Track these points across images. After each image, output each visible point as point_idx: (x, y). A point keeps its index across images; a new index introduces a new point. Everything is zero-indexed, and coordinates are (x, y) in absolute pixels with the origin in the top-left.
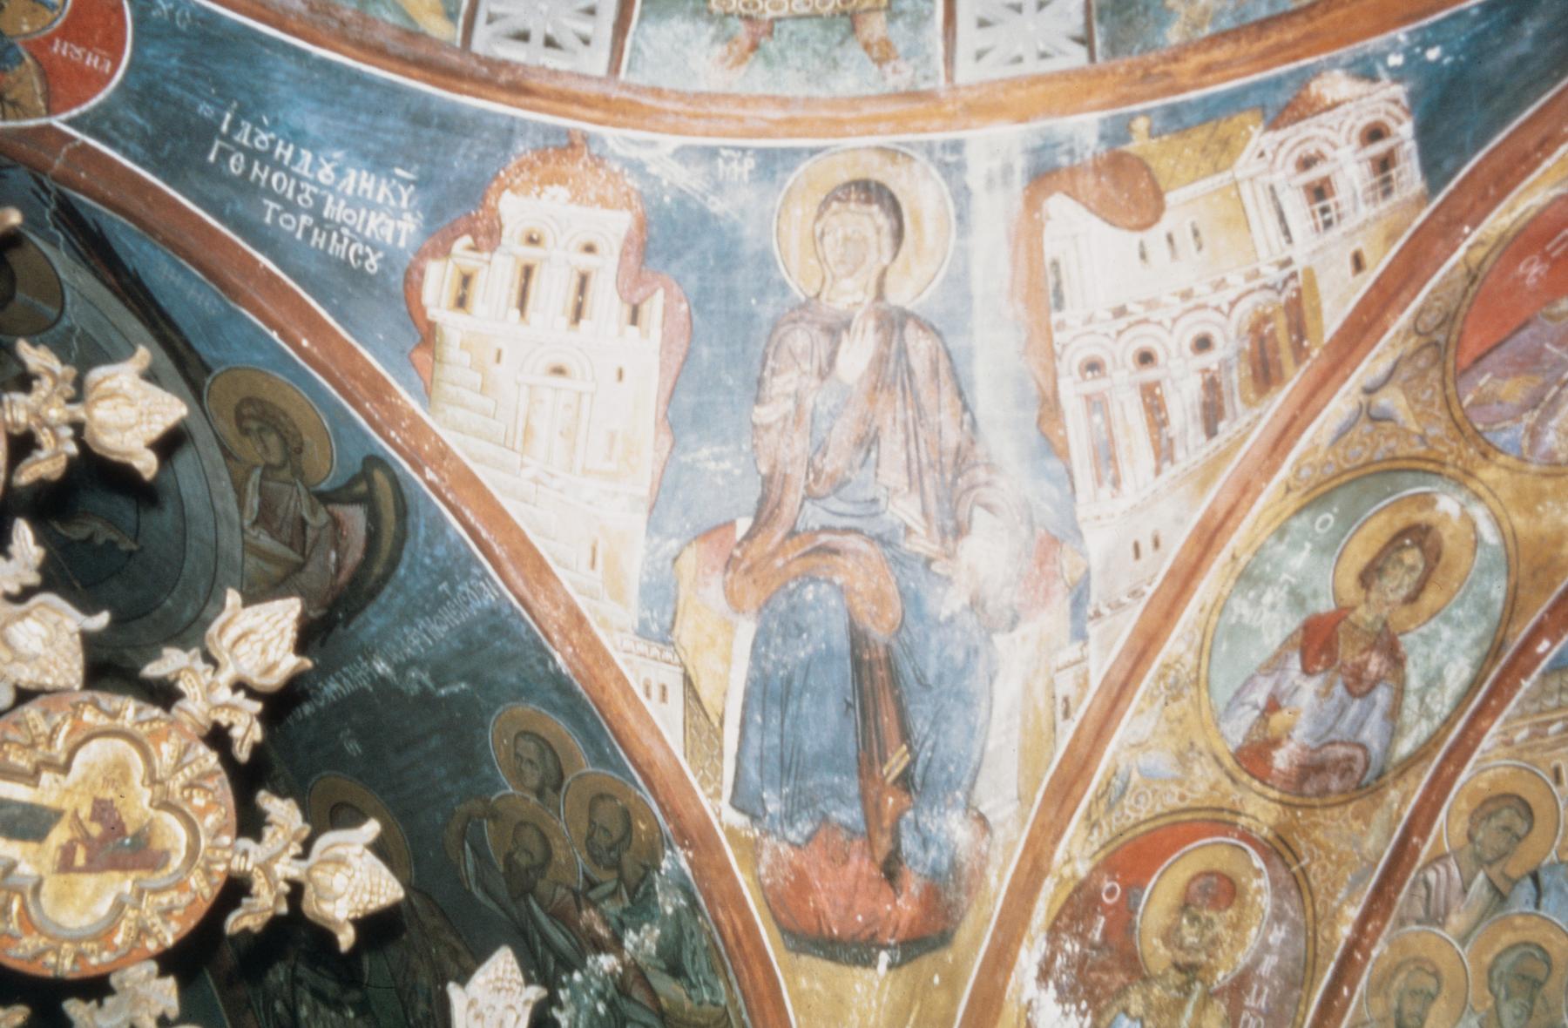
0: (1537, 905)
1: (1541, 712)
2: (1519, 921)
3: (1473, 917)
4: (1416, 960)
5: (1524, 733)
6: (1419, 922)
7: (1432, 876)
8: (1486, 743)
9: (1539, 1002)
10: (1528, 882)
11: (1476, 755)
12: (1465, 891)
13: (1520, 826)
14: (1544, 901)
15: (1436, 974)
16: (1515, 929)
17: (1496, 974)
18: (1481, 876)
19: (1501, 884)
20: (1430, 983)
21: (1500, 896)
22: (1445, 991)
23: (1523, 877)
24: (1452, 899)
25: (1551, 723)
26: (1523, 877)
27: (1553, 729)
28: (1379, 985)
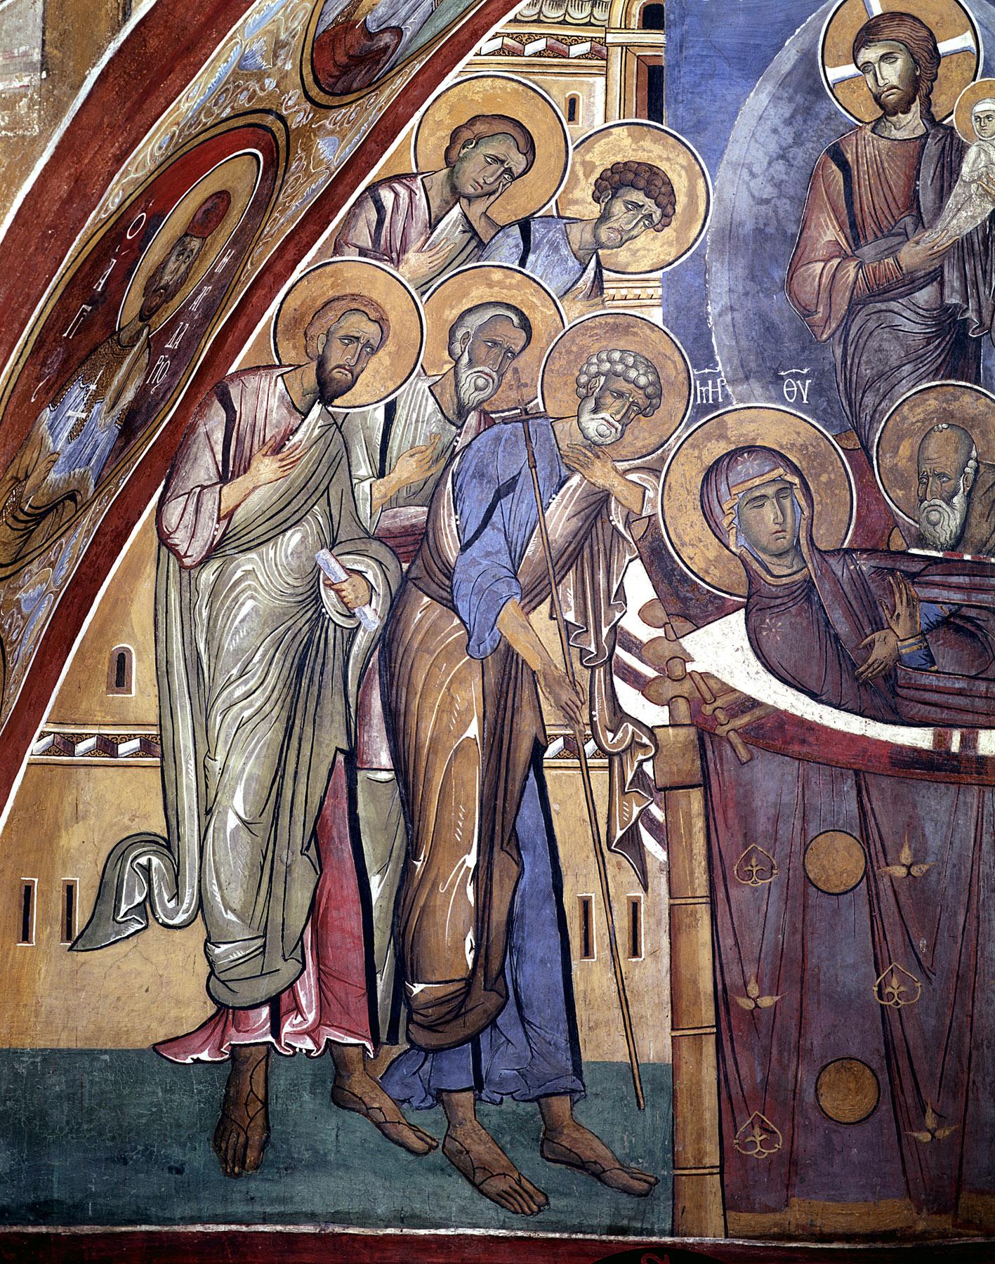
0: (523, 263)
1: (564, 23)
2: (497, 275)
3: (439, 260)
4: (354, 297)
5: (540, 45)
6: (363, 252)
7: (387, 196)
8: (485, 44)
9: (509, 375)
10: (516, 231)
11: (469, 57)
12: (432, 225)
13: (517, 161)
14: (531, 258)
15: (381, 322)
16: (490, 286)
17: (459, 334)
18: (456, 212)
19: (480, 226)
20: (373, 329)
21: (476, 243)
22: (390, 346)
23: (511, 225)
24: (413, 233)
25: (578, 40)
26: (511, 225)
27: (576, 50)
28: (297, 321)
